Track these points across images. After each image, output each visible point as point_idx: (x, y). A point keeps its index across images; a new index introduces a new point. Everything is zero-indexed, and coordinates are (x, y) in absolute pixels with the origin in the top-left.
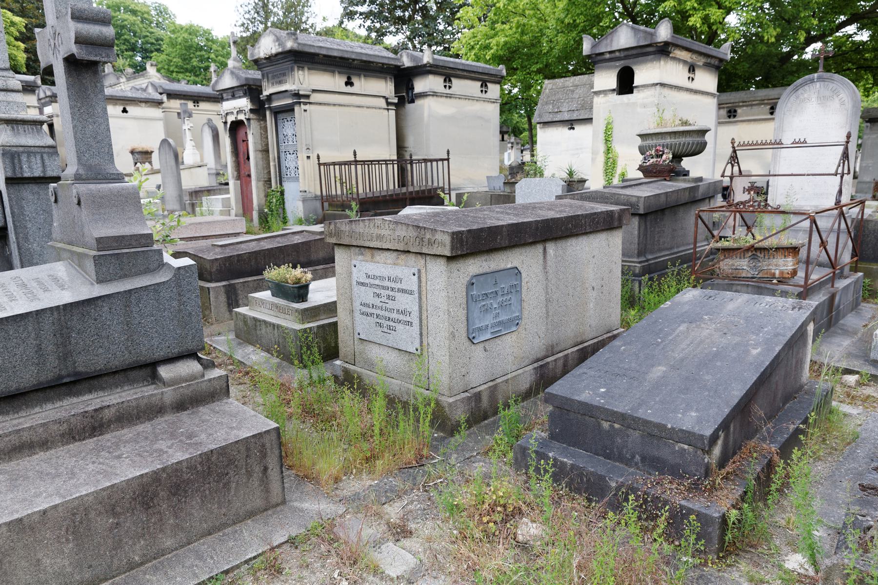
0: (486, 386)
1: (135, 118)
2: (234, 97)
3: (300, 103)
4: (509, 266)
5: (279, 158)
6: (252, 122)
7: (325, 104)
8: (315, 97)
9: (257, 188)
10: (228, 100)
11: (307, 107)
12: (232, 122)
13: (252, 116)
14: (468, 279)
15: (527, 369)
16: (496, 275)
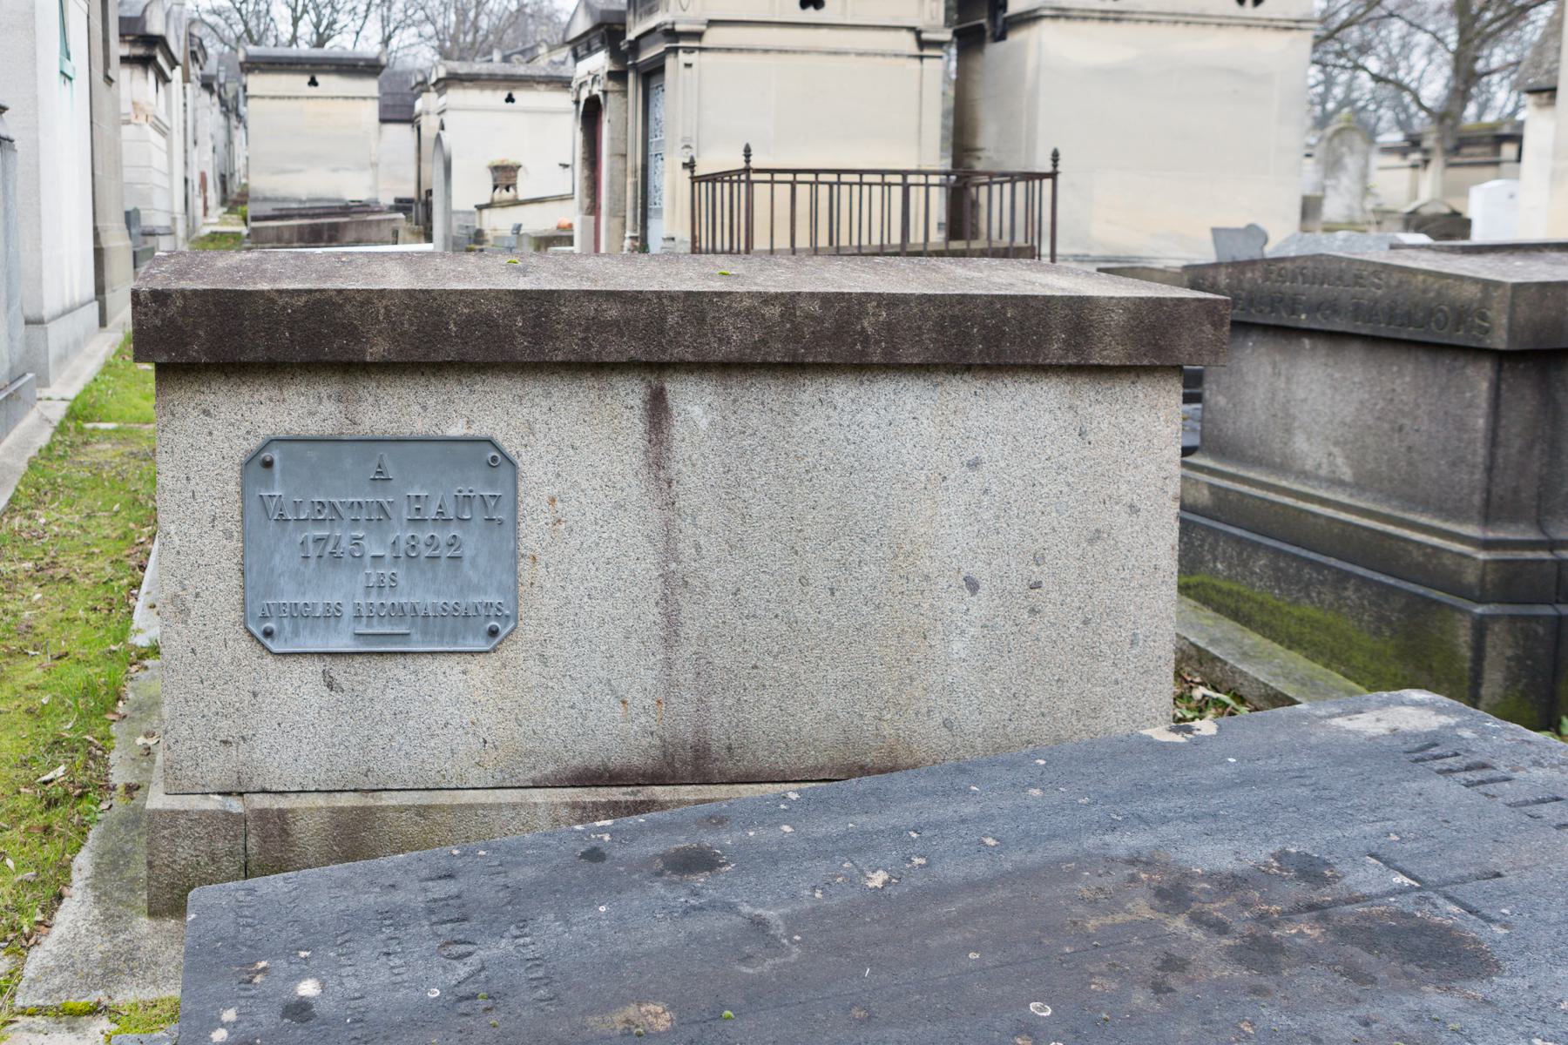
0: (320, 801)
1: (526, 111)
2: (590, 51)
3: (675, 50)
4: (457, 430)
5: (645, 168)
6: (610, 96)
7: (741, 50)
8: (713, 37)
9: (608, 230)
10: (582, 58)
11: (693, 58)
12: (587, 101)
13: (611, 85)
14: (254, 443)
15: (539, 796)
16: (384, 451)
